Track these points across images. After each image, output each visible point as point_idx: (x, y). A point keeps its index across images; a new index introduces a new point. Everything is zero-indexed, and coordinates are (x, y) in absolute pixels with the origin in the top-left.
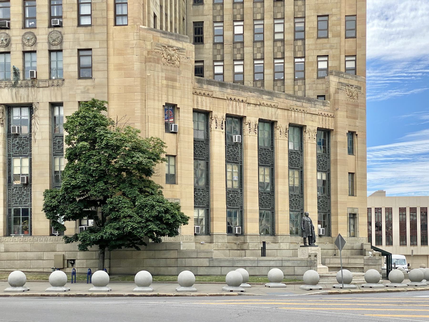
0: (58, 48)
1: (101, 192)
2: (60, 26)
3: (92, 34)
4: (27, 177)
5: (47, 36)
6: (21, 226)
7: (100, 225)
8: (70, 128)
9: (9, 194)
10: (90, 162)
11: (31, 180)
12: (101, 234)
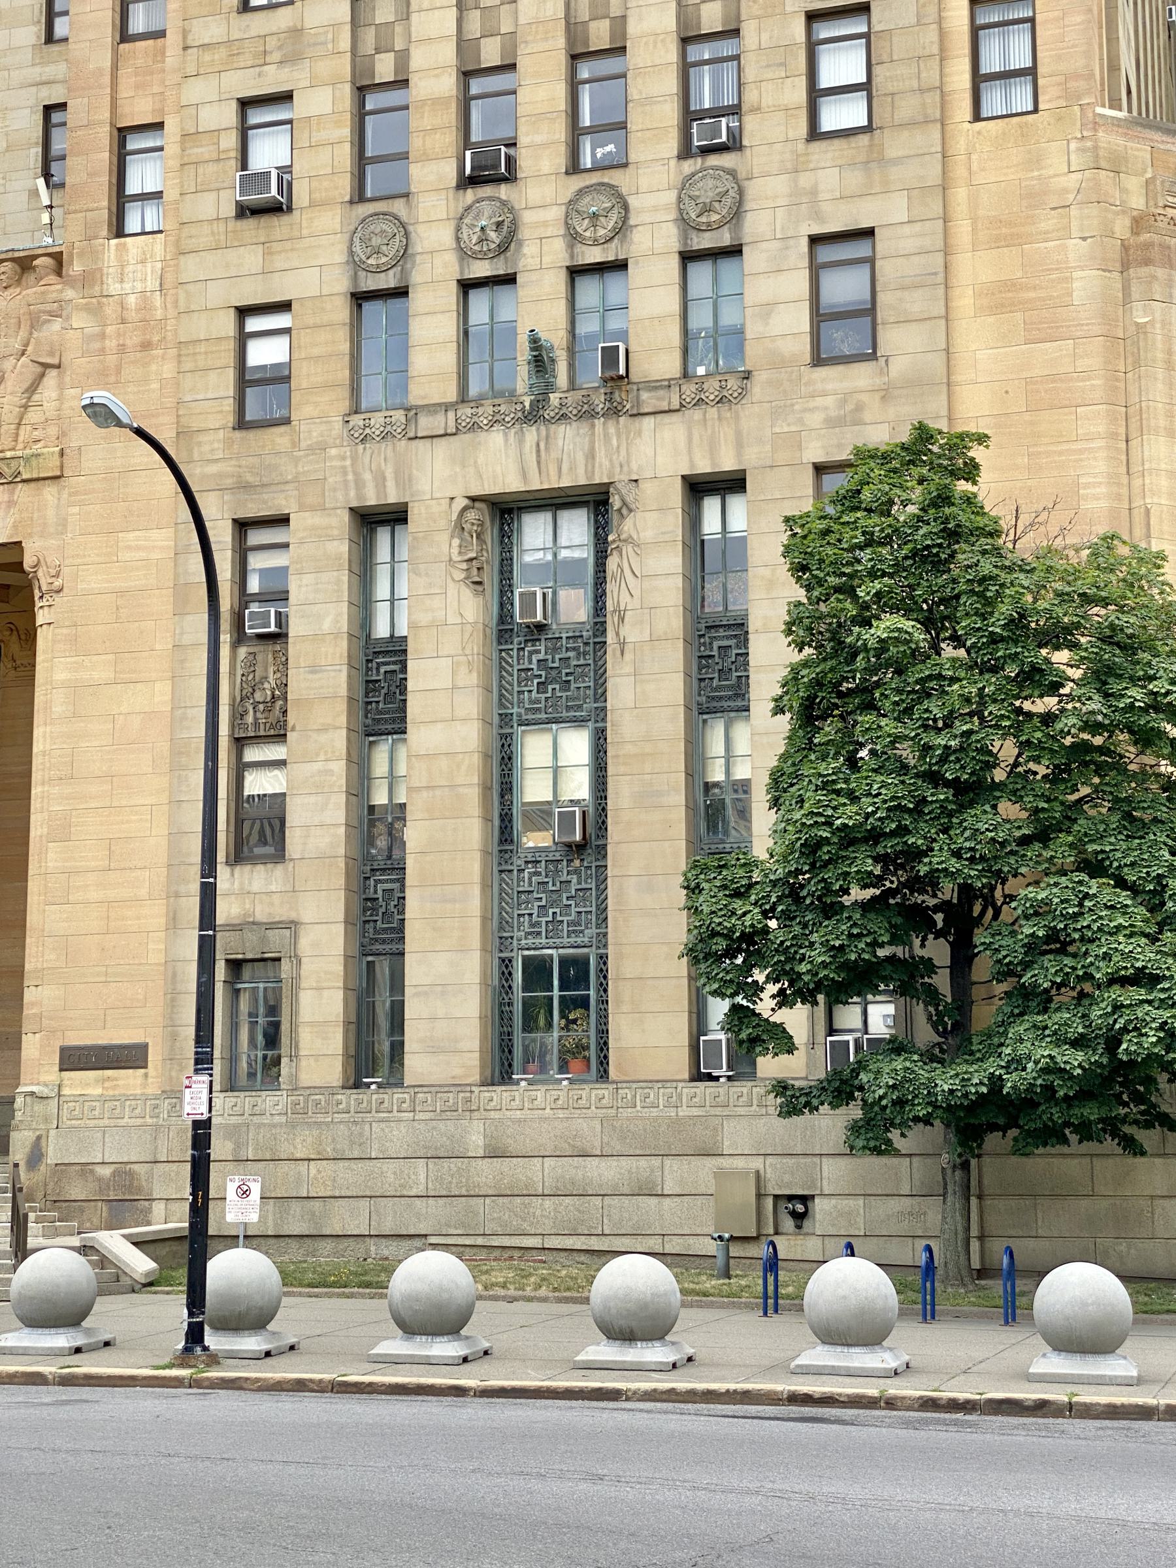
0: (724, 239)
1: (983, 858)
2: (734, 144)
3: (873, 165)
4: (584, 812)
5: (672, 196)
6: (556, 1034)
7: (945, 1029)
8: (821, 561)
9: (502, 890)
10: (927, 710)
11: (602, 826)
12: (992, 1066)
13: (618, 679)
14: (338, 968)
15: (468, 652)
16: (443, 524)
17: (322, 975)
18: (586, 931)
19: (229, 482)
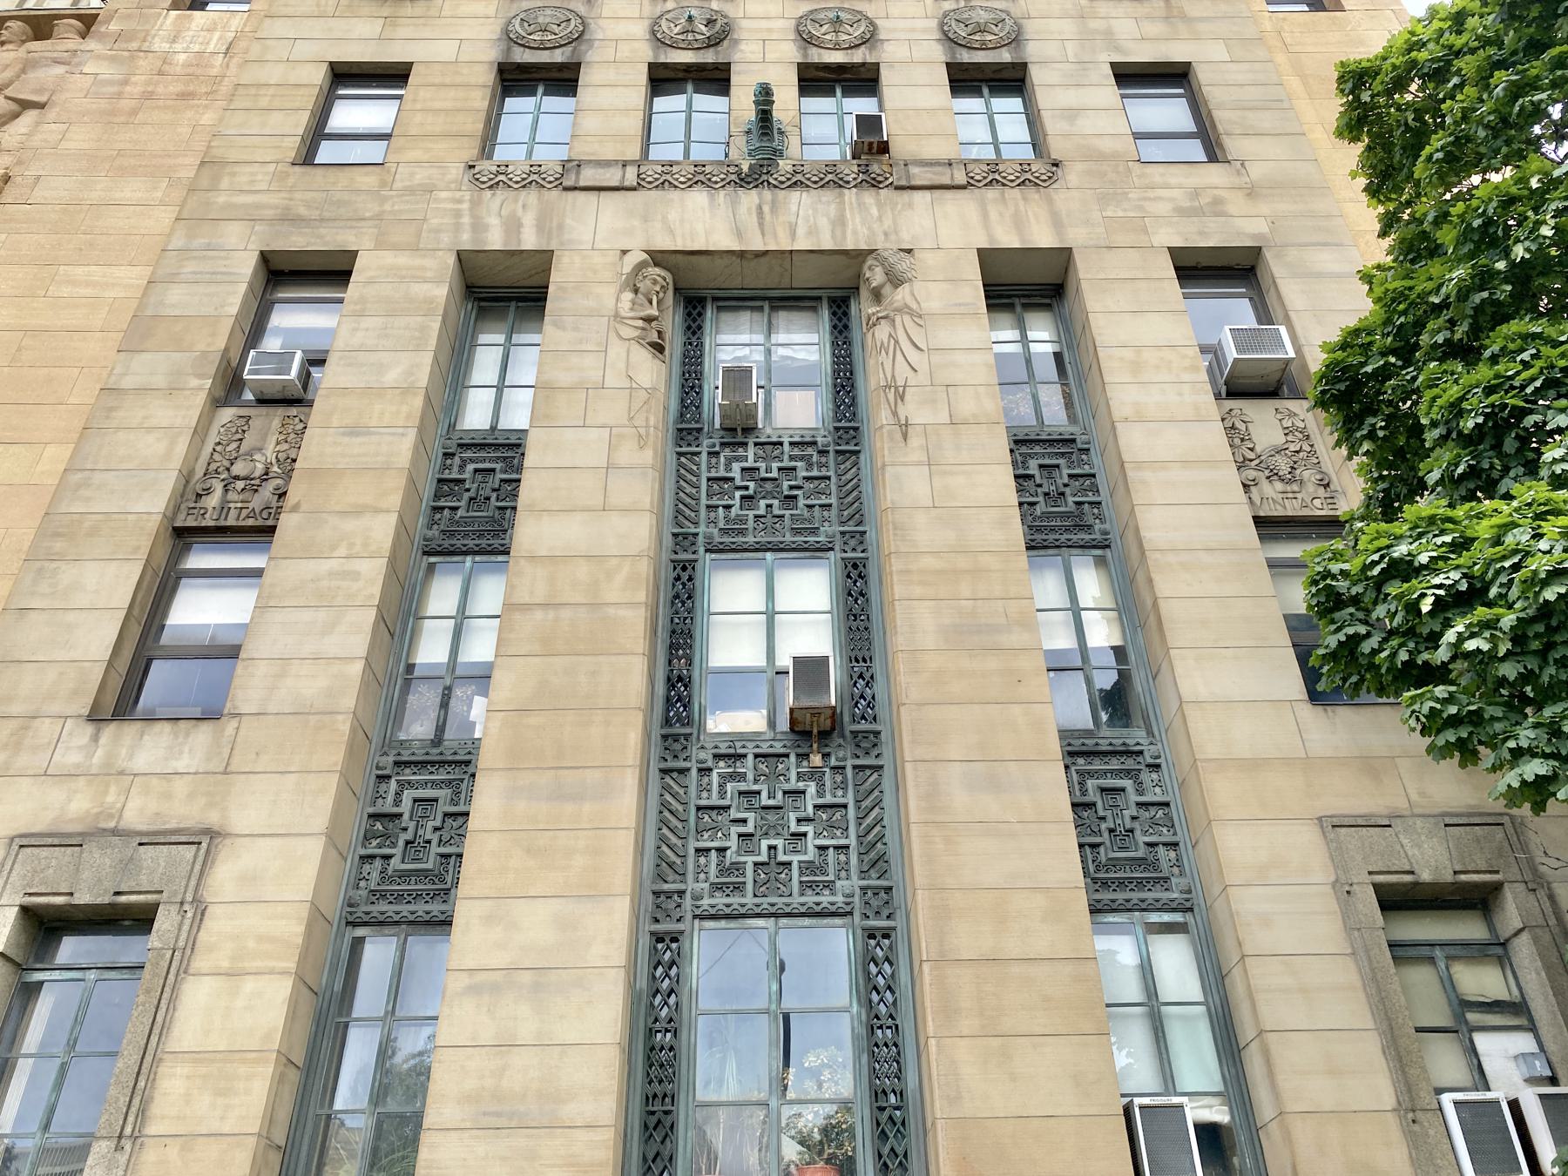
9: (664, 805)
13: (899, 469)
14: (292, 928)
15: (640, 421)
17: (251, 944)
18: (839, 884)
19: (269, 213)
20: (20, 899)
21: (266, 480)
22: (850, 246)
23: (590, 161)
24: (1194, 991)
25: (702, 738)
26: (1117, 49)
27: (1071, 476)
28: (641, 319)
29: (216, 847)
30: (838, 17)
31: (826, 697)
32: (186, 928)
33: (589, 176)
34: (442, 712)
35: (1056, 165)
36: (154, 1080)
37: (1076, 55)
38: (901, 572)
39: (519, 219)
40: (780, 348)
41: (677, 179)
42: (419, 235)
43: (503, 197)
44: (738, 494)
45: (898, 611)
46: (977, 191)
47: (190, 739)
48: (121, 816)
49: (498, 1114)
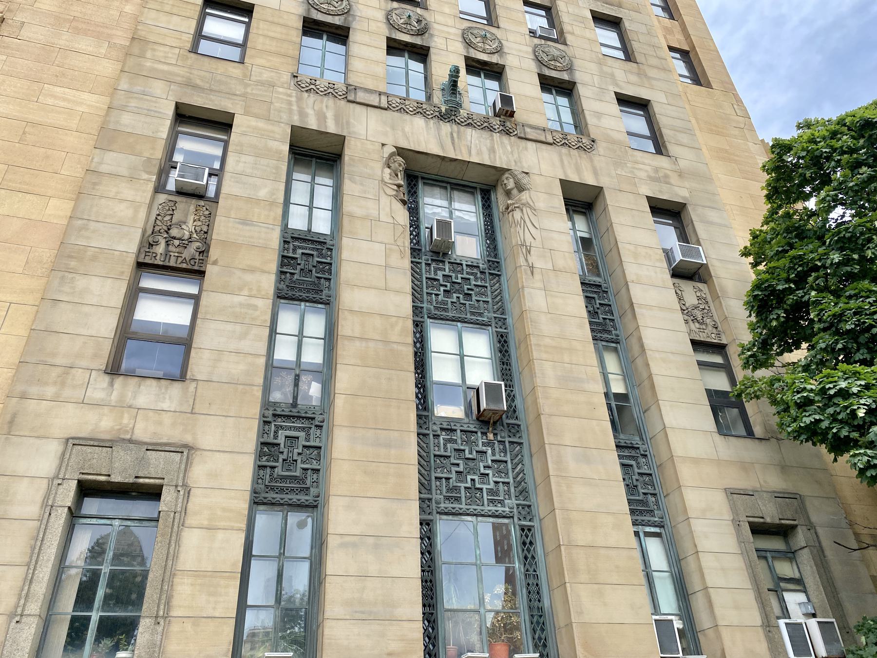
16: (376, 156)
17: (219, 513)
18: (506, 501)
19: (179, 79)
20: (78, 476)
21: (191, 242)
22: (498, 164)
23: (361, 88)
24: (664, 566)
25: (433, 418)
26: (617, 85)
27: (600, 304)
28: (395, 185)
29: (192, 455)
30: (486, 35)
31: (501, 405)
32: (180, 500)
33: (361, 97)
34: (296, 389)
35: (593, 141)
36: (172, 585)
37: (599, 84)
38: (535, 345)
39: (325, 114)
40: (456, 211)
41: (408, 109)
42: (269, 111)
43: (314, 99)
44: (442, 289)
45: (536, 366)
46: (557, 147)
47: (169, 392)
48: (133, 432)
49: (363, 612)
